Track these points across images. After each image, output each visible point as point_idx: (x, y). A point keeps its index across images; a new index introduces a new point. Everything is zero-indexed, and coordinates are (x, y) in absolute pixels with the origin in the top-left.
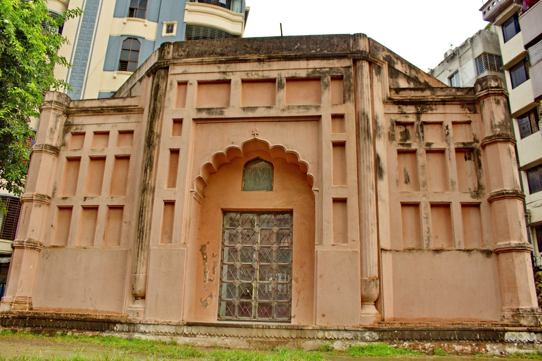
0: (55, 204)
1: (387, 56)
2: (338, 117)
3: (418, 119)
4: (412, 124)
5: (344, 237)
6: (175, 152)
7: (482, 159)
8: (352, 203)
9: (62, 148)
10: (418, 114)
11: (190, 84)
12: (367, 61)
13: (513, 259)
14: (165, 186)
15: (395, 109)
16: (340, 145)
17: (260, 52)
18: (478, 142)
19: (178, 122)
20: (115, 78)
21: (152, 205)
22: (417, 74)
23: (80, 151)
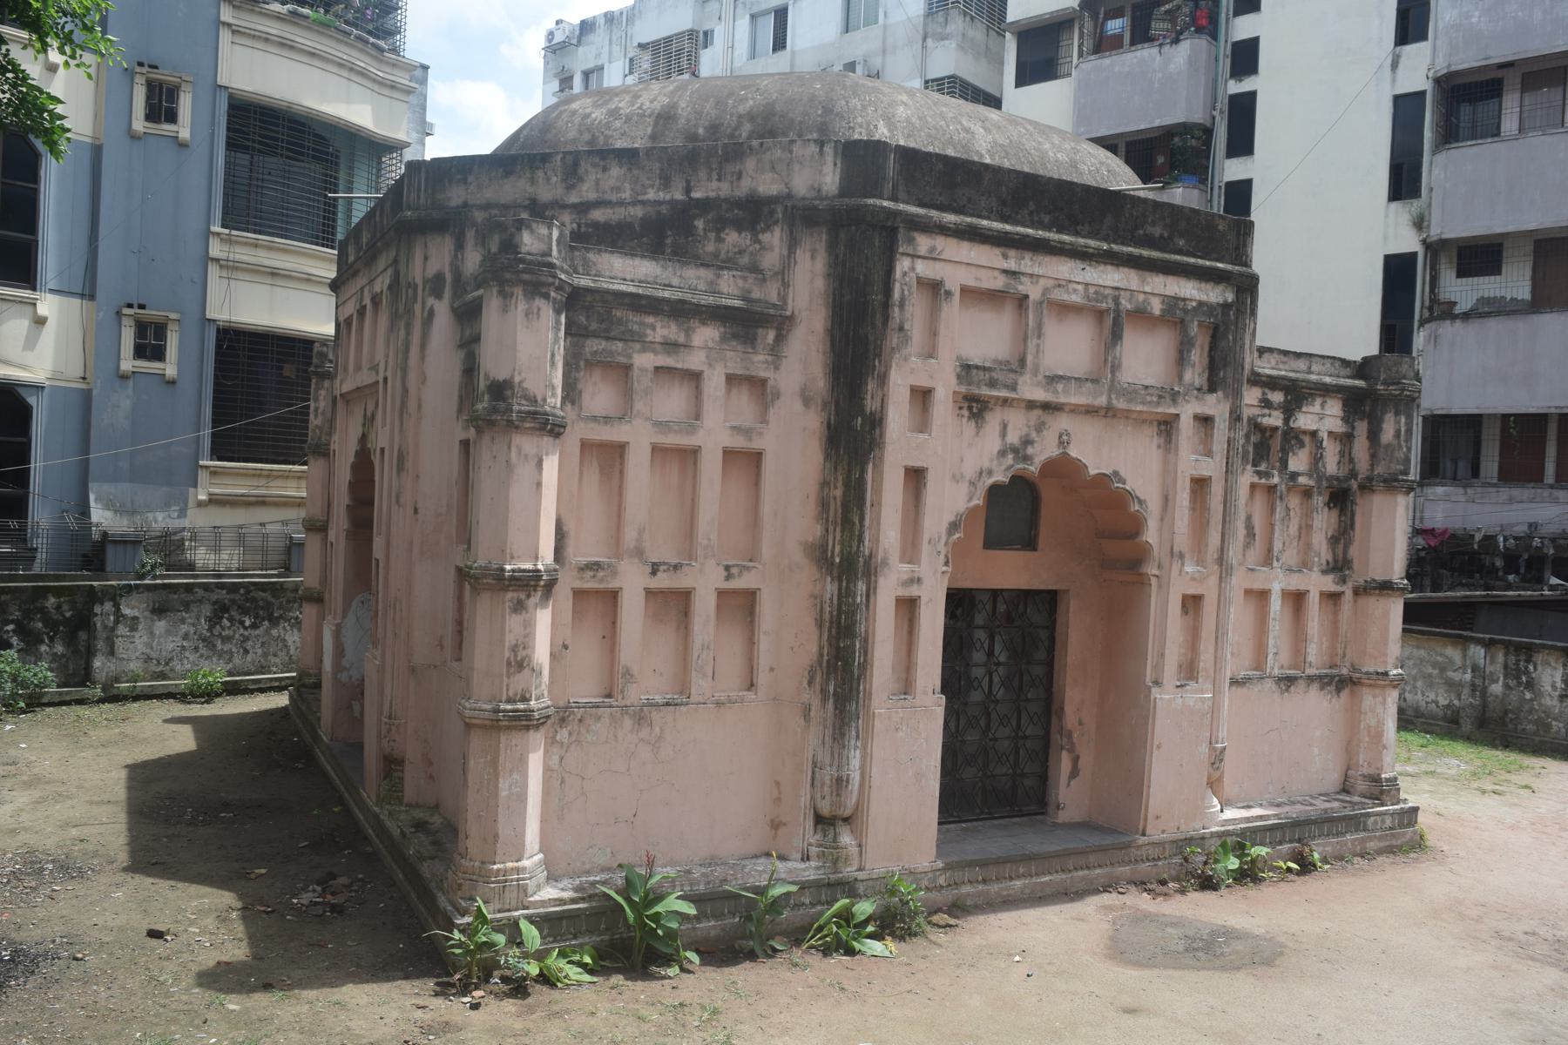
0: (567, 582)
2: (1205, 421)
3: (1286, 421)
4: (1276, 428)
5: (1189, 671)
7: (1358, 510)
8: (1209, 607)
10: (1289, 410)
11: (946, 291)
13: (1385, 700)
14: (898, 559)
16: (1200, 485)
17: (1078, 228)
18: (1356, 479)
19: (922, 396)
21: (867, 606)
23: (625, 427)
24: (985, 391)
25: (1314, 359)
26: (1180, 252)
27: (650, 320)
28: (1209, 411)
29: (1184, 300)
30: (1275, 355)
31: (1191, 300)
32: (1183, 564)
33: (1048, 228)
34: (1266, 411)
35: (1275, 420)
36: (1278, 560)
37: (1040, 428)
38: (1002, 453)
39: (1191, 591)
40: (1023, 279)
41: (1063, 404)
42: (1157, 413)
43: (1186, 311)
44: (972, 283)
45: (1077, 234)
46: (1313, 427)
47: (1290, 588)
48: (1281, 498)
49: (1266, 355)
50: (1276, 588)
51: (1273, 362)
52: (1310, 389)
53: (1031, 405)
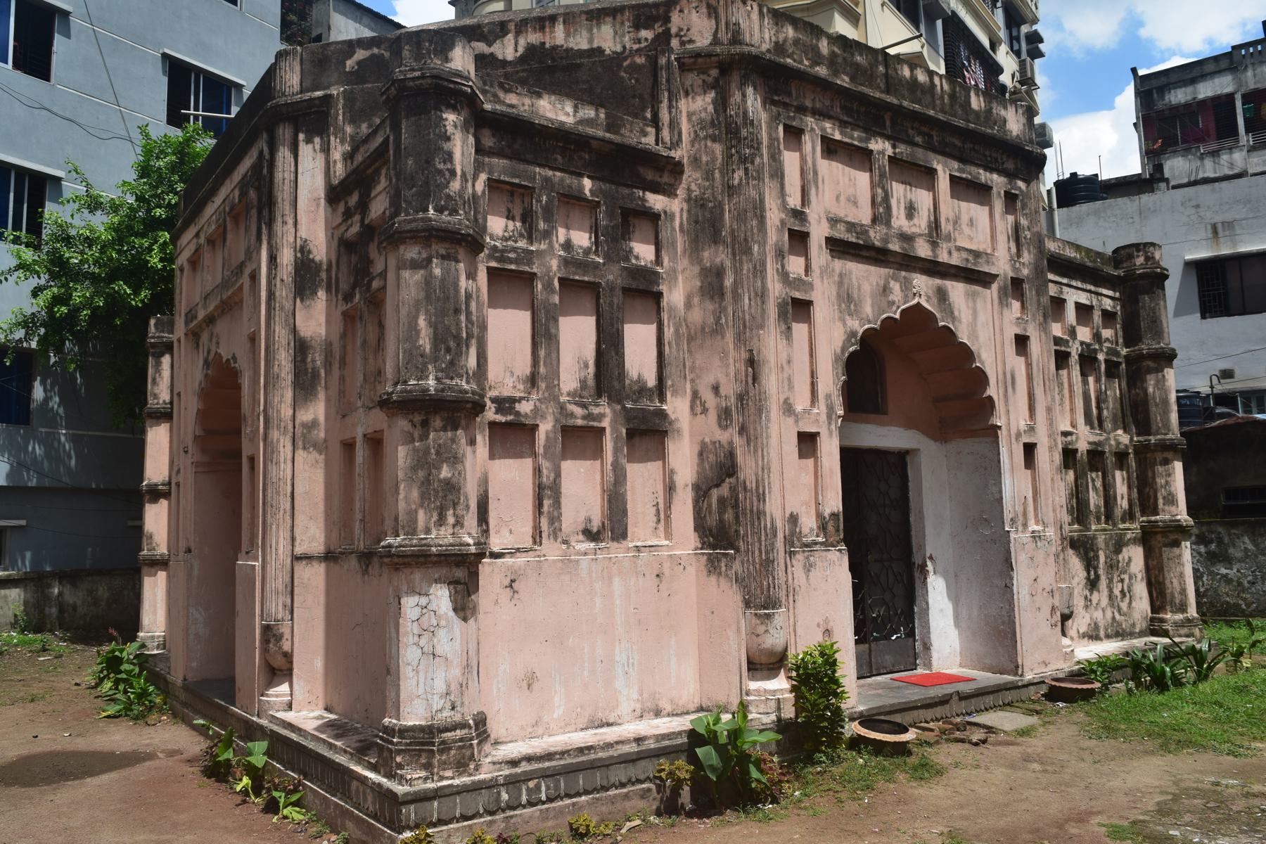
1: (359, 63)
22: (490, 45)
50: (359, 432)
52: (369, 166)
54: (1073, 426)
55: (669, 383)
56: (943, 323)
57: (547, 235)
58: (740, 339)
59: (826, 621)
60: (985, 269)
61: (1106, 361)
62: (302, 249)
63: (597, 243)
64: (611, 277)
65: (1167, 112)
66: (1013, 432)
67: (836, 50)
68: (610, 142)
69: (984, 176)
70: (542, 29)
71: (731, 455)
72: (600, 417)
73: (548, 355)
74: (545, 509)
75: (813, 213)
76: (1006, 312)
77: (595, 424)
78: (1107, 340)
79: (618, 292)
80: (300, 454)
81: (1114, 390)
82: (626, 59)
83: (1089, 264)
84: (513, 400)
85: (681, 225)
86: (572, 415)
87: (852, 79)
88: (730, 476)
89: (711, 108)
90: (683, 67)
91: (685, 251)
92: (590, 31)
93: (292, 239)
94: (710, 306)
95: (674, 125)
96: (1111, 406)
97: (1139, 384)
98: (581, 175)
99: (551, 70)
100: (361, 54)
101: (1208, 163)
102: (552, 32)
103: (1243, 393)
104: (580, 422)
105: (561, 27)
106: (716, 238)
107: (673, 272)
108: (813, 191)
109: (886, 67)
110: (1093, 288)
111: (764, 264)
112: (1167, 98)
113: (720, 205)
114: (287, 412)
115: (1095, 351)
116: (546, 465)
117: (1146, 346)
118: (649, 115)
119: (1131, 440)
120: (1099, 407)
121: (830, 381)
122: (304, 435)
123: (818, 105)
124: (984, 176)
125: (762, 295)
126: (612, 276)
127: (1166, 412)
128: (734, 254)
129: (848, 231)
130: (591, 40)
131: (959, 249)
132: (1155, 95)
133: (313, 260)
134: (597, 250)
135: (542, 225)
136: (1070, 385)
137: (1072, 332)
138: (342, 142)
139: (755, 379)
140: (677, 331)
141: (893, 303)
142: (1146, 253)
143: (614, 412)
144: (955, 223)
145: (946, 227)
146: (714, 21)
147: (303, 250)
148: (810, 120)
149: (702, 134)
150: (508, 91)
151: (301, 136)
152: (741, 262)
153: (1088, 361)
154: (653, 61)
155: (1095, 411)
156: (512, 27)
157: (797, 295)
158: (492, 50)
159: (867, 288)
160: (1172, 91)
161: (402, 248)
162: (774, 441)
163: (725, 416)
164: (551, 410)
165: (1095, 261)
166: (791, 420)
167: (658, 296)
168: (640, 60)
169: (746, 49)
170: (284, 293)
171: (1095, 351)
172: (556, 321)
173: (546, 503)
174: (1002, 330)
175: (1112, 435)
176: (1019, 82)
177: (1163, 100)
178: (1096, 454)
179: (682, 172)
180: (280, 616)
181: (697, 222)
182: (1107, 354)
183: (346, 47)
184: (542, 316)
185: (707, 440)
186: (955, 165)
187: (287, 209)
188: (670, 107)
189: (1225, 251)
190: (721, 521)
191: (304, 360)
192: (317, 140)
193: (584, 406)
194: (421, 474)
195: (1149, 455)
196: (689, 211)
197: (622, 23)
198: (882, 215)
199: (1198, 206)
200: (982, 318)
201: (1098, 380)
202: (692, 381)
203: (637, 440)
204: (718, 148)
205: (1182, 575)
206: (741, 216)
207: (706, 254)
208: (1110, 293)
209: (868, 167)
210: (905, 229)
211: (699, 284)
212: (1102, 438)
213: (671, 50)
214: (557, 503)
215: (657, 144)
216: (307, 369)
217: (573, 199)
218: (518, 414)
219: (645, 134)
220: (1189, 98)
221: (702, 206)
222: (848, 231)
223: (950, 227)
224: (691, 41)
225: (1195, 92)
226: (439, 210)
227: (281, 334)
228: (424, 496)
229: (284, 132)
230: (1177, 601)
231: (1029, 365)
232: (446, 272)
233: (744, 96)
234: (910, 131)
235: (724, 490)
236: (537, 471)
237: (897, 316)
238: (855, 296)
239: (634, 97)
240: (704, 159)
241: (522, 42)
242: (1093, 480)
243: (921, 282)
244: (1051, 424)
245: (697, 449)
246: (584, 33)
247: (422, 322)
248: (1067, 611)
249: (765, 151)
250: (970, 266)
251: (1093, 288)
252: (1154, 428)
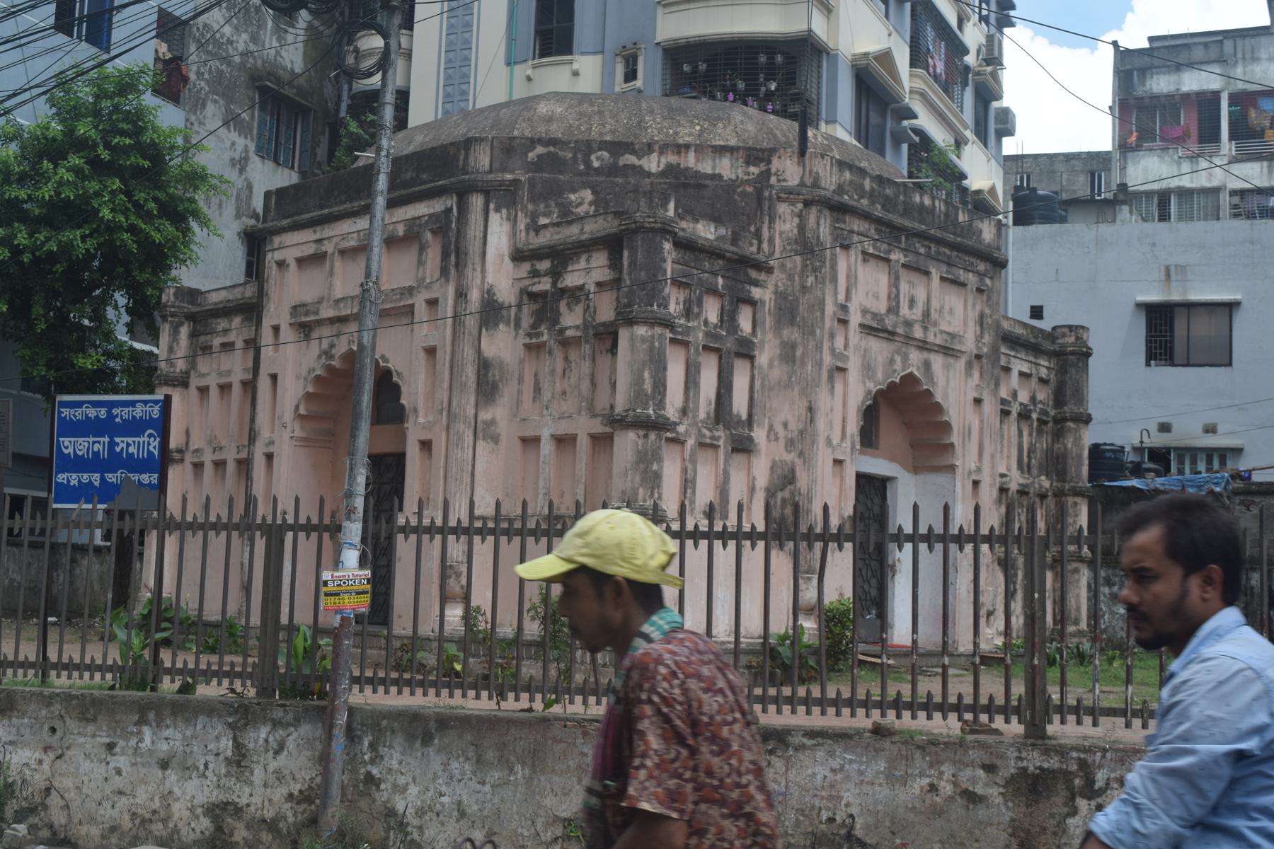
1: (538, 156)
4: (547, 291)
6: (274, 377)
9: (192, 373)
10: (556, 274)
12: (477, 191)
15: (526, 266)
16: (431, 352)
20: (529, 79)
22: (639, 159)
24: (304, 319)
25: (586, 221)
26: (425, 183)
27: (219, 320)
28: (434, 296)
29: (419, 218)
30: (550, 229)
31: (424, 216)
32: (417, 417)
33: (343, 203)
34: (536, 280)
35: (545, 285)
36: (547, 409)
37: (338, 335)
38: (320, 357)
39: (425, 436)
40: (325, 242)
41: (347, 316)
42: (404, 306)
43: (420, 226)
44: (299, 254)
45: (361, 199)
46: (581, 283)
47: (559, 433)
48: (550, 353)
49: (542, 232)
50: (545, 434)
51: (548, 235)
53: (332, 321)
54: (1009, 470)
55: (756, 418)
56: (925, 387)
57: (698, 315)
58: (804, 392)
59: (841, 587)
60: (958, 347)
61: (1038, 420)
62: (489, 292)
63: (721, 320)
64: (729, 345)
65: (1147, 101)
66: (966, 471)
67: (875, 186)
68: (736, 254)
69: (962, 275)
70: (679, 153)
71: (793, 471)
72: (718, 439)
73: (694, 395)
74: (688, 495)
75: (853, 307)
76: (970, 381)
77: (715, 442)
78: (1041, 402)
79: (732, 355)
80: (480, 444)
81: (1043, 444)
82: (739, 186)
83: (1033, 340)
84: (676, 424)
85: (769, 309)
86: (704, 436)
87: (883, 207)
88: (790, 483)
89: (796, 231)
90: (779, 199)
91: (771, 328)
92: (714, 160)
93: (479, 282)
94: (785, 368)
95: (771, 240)
96: (1038, 455)
97: (1061, 440)
98: (717, 275)
99: (686, 186)
100: (540, 150)
101: (1186, 167)
102: (686, 157)
103: (1176, 449)
104: (708, 441)
105: (693, 154)
106: (792, 322)
107: (763, 341)
108: (854, 291)
109: (905, 195)
110: (1033, 360)
111: (822, 343)
112: (1148, 83)
113: (797, 300)
114: (471, 411)
115: (1030, 411)
116: (690, 467)
117: (1069, 409)
118: (752, 229)
119: (1051, 485)
120: (1029, 457)
121: (853, 426)
122: (484, 430)
123: (861, 229)
124: (962, 275)
125: (819, 363)
126: (729, 344)
127: (1080, 464)
128: (804, 334)
129: (873, 319)
130: (714, 168)
131: (942, 332)
132: (1135, 78)
133: (496, 301)
134: (721, 326)
135: (696, 310)
136: (1009, 438)
137: (1015, 394)
138: (526, 216)
139: (812, 421)
140: (762, 383)
141: (895, 371)
142: (1077, 333)
143: (726, 435)
144: (940, 311)
145: (934, 315)
146: (801, 169)
147: (490, 292)
148: (856, 238)
149: (788, 248)
150: (682, 219)
151: (492, 206)
152: (808, 341)
153: (1024, 416)
154: (759, 193)
155: (1026, 459)
156: (656, 148)
157: (840, 364)
158: (640, 163)
159: (880, 360)
160: (1155, 77)
161: (635, 327)
162: (820, 463)
163: (790, 444)
164: (694, 431)
165: (1036, 337)
166: (830, 450)
167: (751, 358)
168: (749, 189)
169: (823, 193)
170: (471, 322)
171: (1030, 411)
172: (699, 372)
173: (689, 491)
174: (965, 393)
175: (1036, 480)
176: (984, 60)
177: (1144, 85)
178: (1023, 492)
179: (772, 273)
180: (460, 559)
181: (780, 309)
182: (1039, 414)
183: (529, 143)
184: (692, 369)
185: (777, 459)
186: (944, 268)
187: (477, 260)
188: (770, 228)
189: (1176, 297)
190: (783, 514)
191: (486, 375)
192: (504, 211)
193: (710, 430)
194: (642, 466)
195: (1063, 499)
196: (775, 300)
197: (737, 159)
198: (893, 309)
199: (1154, 245)
200: (952, 384)
201: (1030, 434)
202: (769, 418)
203: (734, 455)
204: (798, 259)
205: (1078, 596)
206: (811, 309)
207: (785, 332)
208: (1046, 364)
209: (887, 272)
210: (907, 316)
211: (778, 352)
212: (1029, 482)
213: (772, 186)
214: (694, 492)
215: (758, 253)
216: (488, 382)
217: (713, 291)
218: (677, 433)
219: (751, 245)
220: (1172, 88)
221: (785, 298)
222: (873, 319)
223: (937, 316)
224: (785, 180)
225: (1179, 84)
226: (659, 306)
227: (468, 353)
228: (643, 479)
229: (477, 201)
230: (1073, 616)
231: (982, 421)
232: (661, 344)
233: (818, 224)
234: (917, 245)
235: (786, 494)
236: (684, 470)
237: (898, 381)
238: (873, 365)
239: (743, 214)
240: (789, 265)
241: (663, 160)
242: (1019, 515)
243: (915, 356)
244: (993, 467)
245: (769, 464)
246: (710, 162)
247: (646, 375)
248: (991, 608)
249: (828, 263)
250: (948, 345)
251: (1033, 360)
252: (1069, 477)
